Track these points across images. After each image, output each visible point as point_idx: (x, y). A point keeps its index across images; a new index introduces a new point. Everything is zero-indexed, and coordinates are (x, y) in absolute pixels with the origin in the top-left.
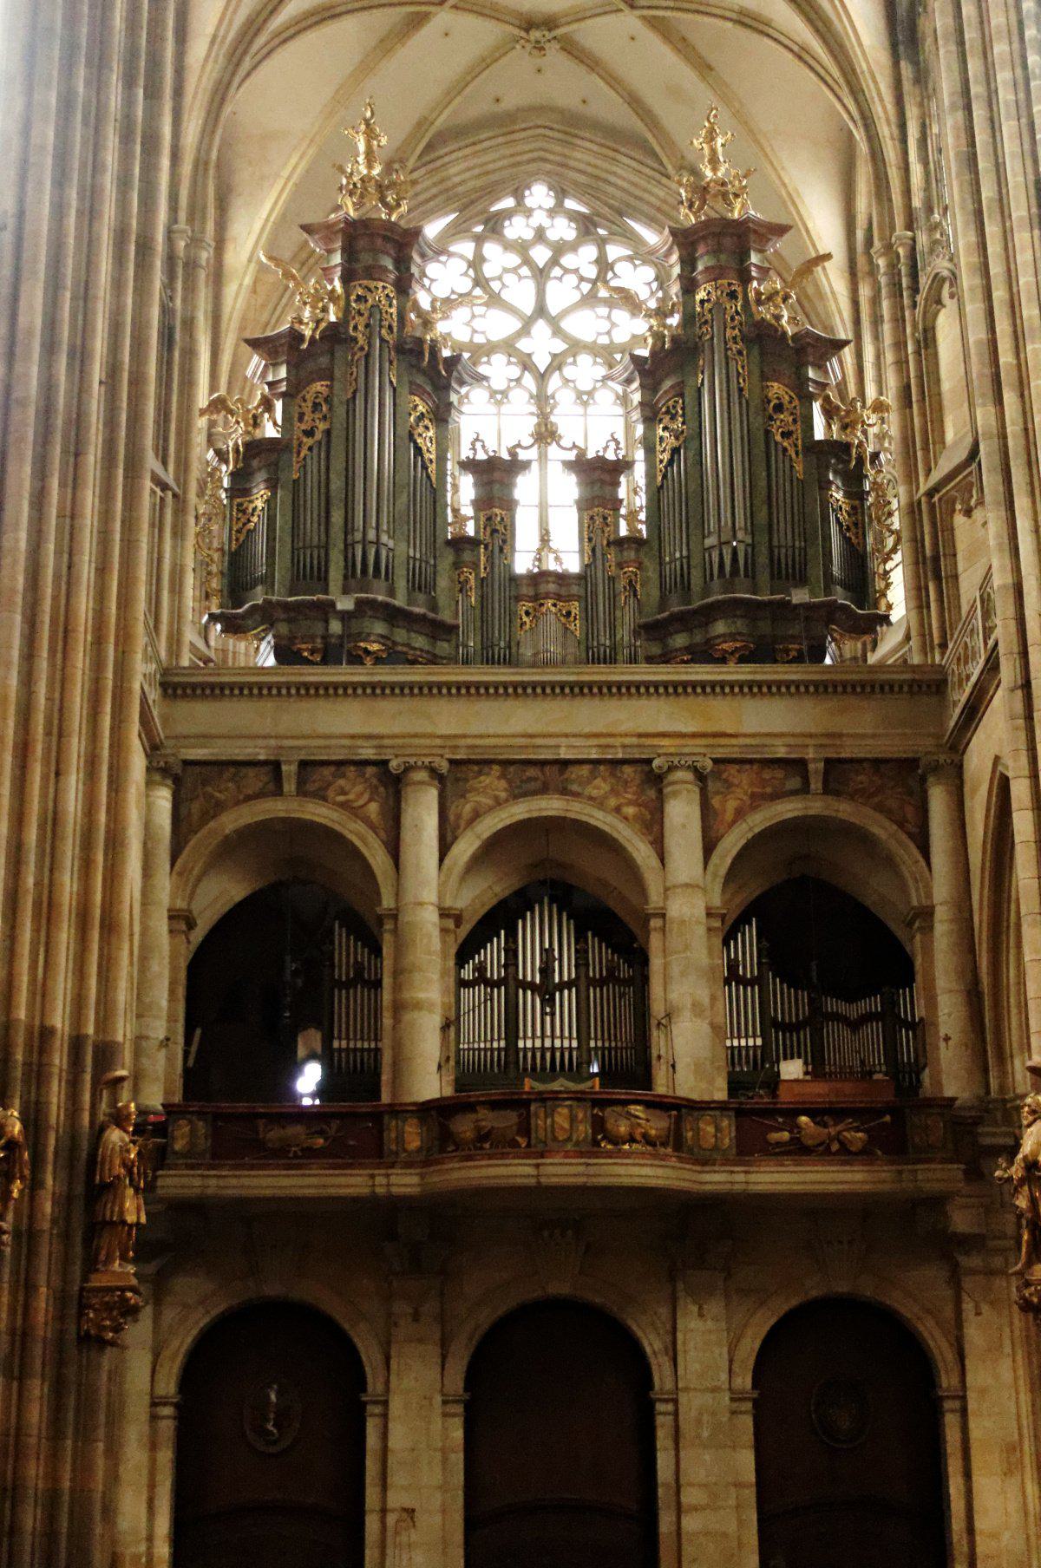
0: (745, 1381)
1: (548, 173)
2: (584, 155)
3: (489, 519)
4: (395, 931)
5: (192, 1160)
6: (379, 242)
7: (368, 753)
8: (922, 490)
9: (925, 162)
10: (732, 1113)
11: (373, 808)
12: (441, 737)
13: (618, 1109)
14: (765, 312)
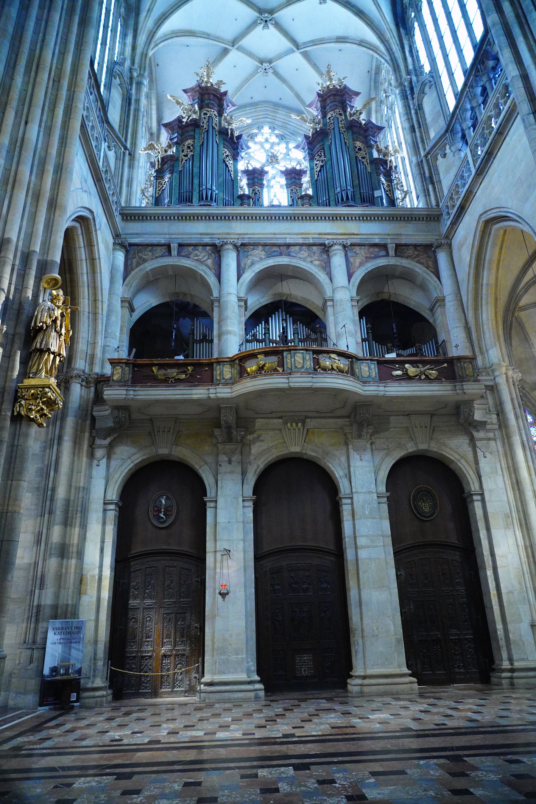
0: (382, 488)
1: (269, 122)
2: (281, 115)
3: (253, 190)
4: (219, 306)
5: (122, 383)
6: (212, 96)
7: (207, 240)
8: (423, 154)
9: (412, 56)
10: (376, 362)
11: (210, 262)
12: (237, 234)
13: (325, 355)
14: (355, 117)
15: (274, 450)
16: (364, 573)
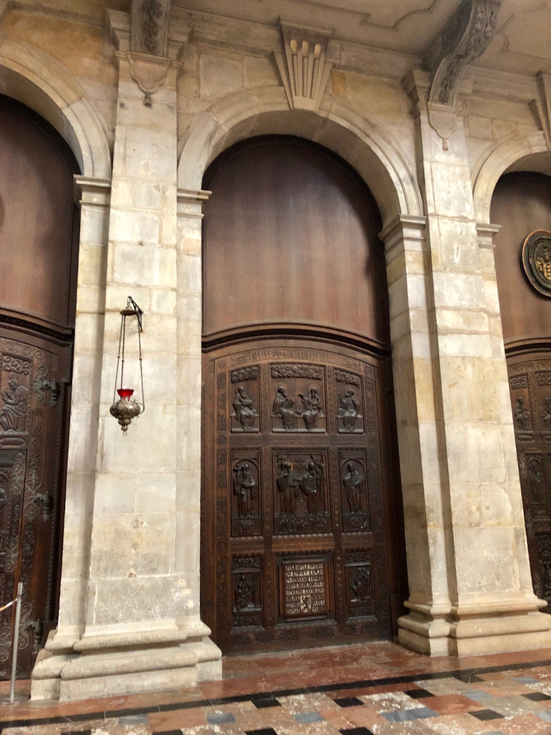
15: (256, 99)
16: (451, 386)
